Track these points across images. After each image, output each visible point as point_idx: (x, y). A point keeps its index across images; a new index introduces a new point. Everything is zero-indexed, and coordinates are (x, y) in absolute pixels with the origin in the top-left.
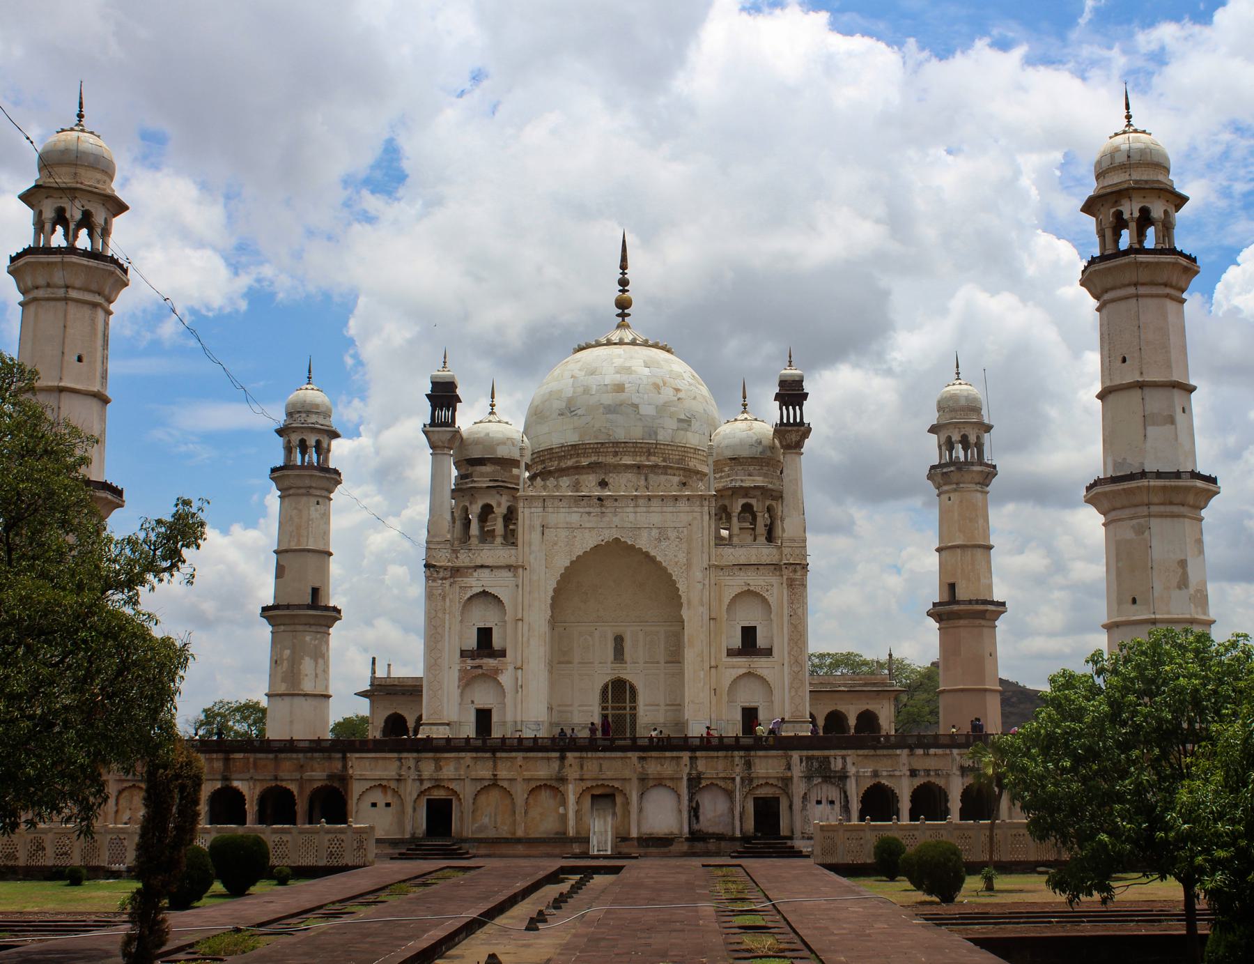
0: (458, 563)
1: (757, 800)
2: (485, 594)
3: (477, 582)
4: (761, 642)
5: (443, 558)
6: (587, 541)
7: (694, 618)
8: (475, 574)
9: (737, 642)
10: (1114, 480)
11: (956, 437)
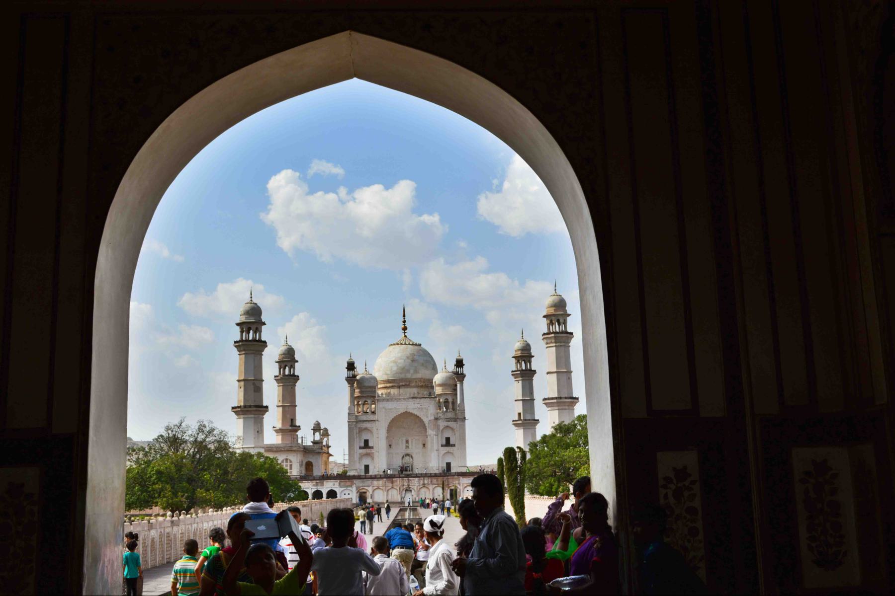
1: (451, 490)
2: (366, 429)
4: (452, 442)
9: (444, 443)
10: (549, 399)
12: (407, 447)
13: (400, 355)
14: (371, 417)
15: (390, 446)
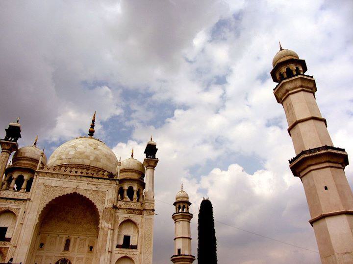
9: (121, 243)
11: (182, 206)
12: (67, 247)
13: (81, 142)
14: (22, 195)
15: (42, 245)
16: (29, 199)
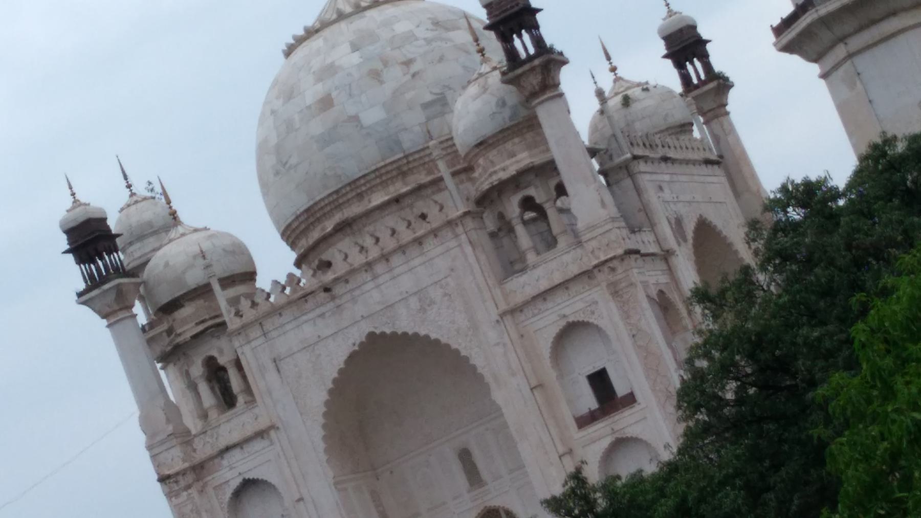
0: (199, 456)
3: (230, 473)
5: (176, 461)
6: (335, 355)
7: (511, 395)
8: (225, 462)
16: (273, 427)
